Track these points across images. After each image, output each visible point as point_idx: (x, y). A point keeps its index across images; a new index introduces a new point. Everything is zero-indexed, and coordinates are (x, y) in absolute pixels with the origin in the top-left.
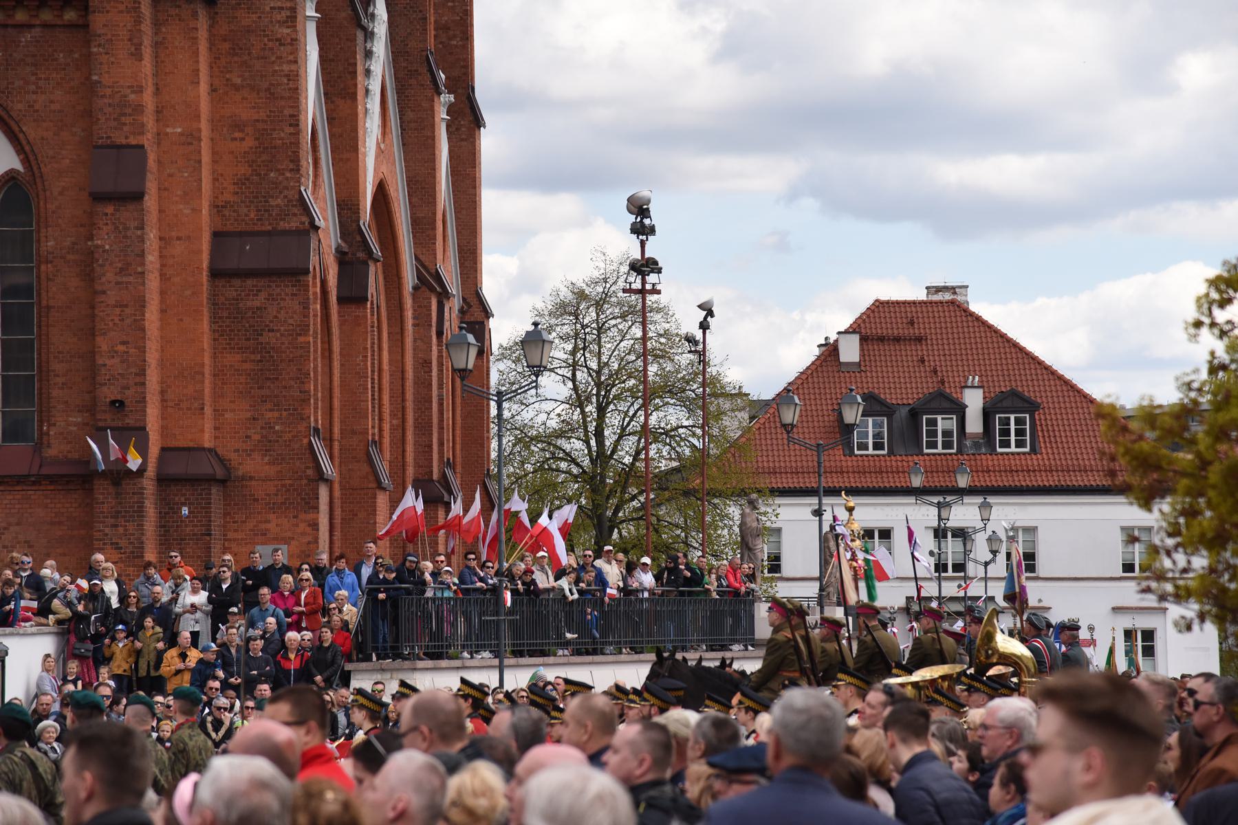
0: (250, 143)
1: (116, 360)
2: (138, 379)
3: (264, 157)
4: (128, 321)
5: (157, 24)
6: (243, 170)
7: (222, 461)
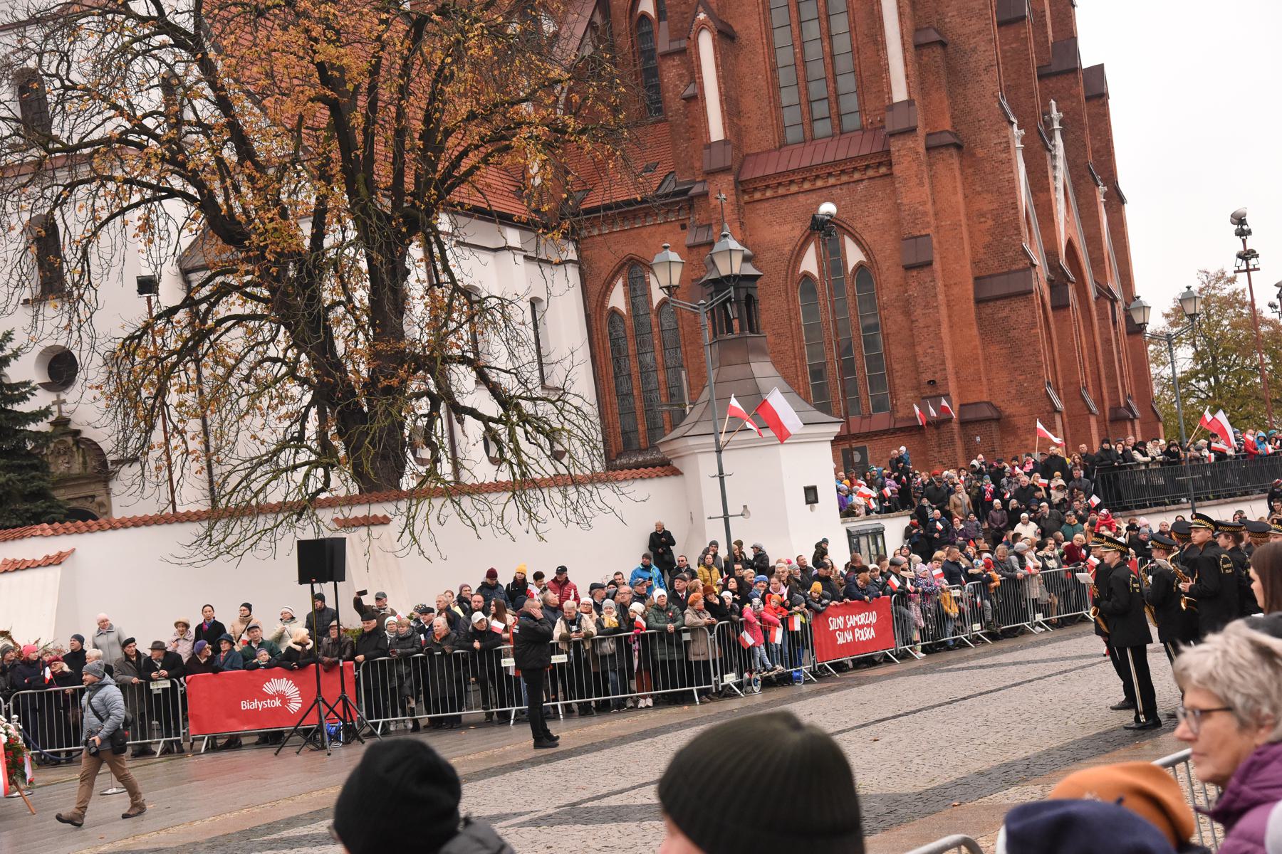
0: (990, 223)
1: (928, 358)
2: (942, 367)
3: (999, 229)
4: (932, 335)
5: (930, 165)
6: (988, 239)
7: (995, 408)
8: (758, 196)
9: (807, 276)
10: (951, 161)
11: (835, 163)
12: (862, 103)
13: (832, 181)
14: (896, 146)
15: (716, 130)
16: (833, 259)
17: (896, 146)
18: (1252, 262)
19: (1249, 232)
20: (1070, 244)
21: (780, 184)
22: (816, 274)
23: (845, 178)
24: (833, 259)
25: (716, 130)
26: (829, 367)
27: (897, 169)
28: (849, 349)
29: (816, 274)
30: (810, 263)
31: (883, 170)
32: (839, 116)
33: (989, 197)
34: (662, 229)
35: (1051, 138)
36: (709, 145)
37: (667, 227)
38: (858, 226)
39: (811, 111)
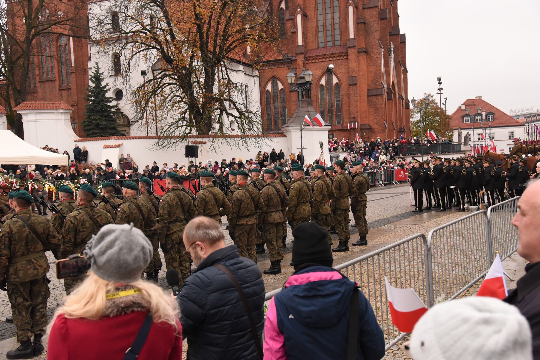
0: (373, 74)
6: (372, 79)
7: (370, 126)
8: (310, 61)
9: (322, 85)
10: (363, 57)
11: (332, 54)
12: (341, 38)
13: (331, 59)
14: (349, 51)
15: (300, 42)
16: (329, 81)
17: (349, 51)
18: (442, 91)
19: (441, 83)
20: (393, 82)
21: (316, 59)
22: (324, 85)
23: (335, 59)
24: (329, 81)
25: (300, 42)
26: (326, 111)
27: (349, 57)
28: (332, 107)
29: (324, 85)
30: (323, 82)
31: (345, 57)
32: (334, 41)
33: (373, 67)
34: (283, 68)
35: (391, 52)
36: (298, 46)
37: (284, 68)
38: (337, 72)
39: (327, 39)
